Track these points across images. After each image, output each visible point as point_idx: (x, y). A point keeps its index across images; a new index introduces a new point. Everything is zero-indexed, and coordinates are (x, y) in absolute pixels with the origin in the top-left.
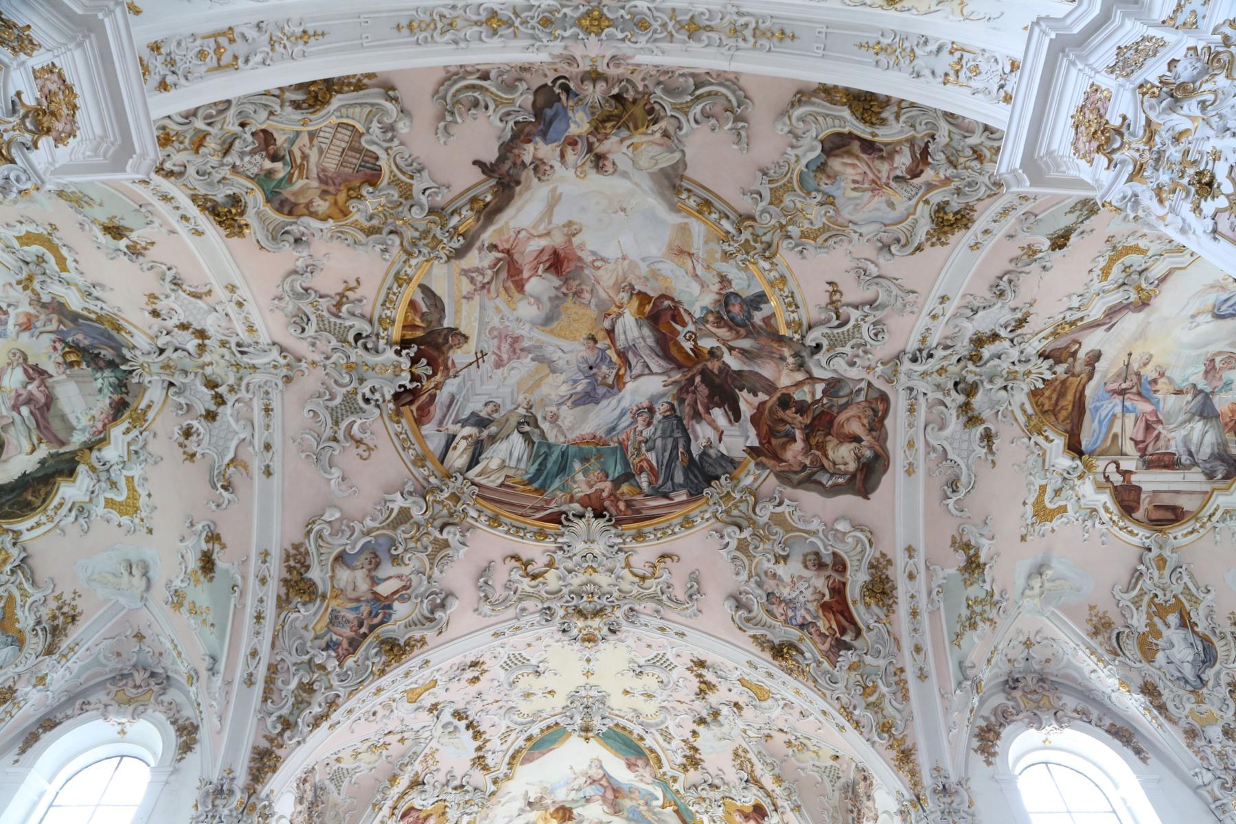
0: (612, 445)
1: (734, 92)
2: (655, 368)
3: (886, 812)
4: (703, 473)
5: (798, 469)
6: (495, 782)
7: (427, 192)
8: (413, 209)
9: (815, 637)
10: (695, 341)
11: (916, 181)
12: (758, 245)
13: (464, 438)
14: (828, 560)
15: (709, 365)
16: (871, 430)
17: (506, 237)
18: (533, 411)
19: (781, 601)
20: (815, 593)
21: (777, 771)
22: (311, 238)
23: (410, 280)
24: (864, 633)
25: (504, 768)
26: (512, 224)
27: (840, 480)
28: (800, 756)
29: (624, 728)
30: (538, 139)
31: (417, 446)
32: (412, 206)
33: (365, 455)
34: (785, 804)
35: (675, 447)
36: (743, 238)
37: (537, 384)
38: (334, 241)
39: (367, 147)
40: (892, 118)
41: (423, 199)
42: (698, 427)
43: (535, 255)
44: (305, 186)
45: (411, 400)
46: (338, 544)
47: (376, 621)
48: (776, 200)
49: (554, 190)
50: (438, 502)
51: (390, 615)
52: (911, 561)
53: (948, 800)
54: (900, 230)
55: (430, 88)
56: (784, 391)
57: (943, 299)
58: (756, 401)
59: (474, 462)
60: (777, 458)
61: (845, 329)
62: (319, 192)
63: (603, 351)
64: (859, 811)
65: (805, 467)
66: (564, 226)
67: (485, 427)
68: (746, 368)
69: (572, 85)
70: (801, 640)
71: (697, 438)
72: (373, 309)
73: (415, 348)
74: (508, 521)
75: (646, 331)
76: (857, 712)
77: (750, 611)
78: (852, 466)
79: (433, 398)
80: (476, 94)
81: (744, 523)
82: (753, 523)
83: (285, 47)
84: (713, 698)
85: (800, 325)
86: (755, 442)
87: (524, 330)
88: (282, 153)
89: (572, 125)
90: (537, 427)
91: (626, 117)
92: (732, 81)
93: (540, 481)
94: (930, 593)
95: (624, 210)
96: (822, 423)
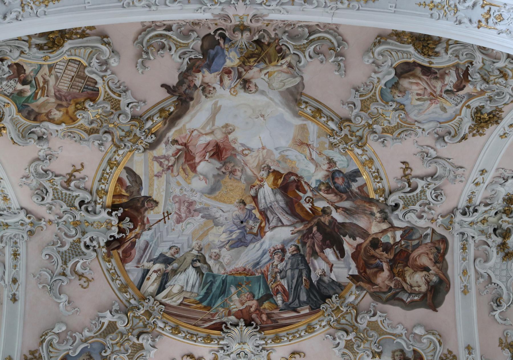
0: (257, 275)
1: (335, 37)
4: (320, 294)
5: (385, 290)
7: (130, 106)
8: (121, 117)
10: (312, 203)
11: (461, 93)
12: (353, 138)
13: (155, 271)
15: (322, 219)
16: (436, 262)
17: (184, 135)
18: (203, 252)
22: (50, 136)
23: (119, 164)
26: (188, 126)
27: (416, 298)
30: (204, 70)
31: (122, 278)
32: (120, 115)
33: (85, 285)
35: (300, 276)
36: (343, 133)
37: (205, 234)
38: (66, 138)
39: (89, 75)
40: (442, 51)
41: (128, 110)
42: (315, 262)
43: (204, 146)
44: (45, 101)
45: (118, 246)
48: (365, 108)
49: (216, 104)
50: (136, 317)
54: (450, 126)
55: (132, 37)
56: (374, 236)
57: (483, 172)
58: (355, 243)
59: (162, 288)
61: (415, 193)
62: (55, 105)
63: (250, 211)
65: (390, 289)
66: (223, 127)
67: (170, 264)
68: (347, 221)
69: (227, 34)
71: (315, 269)
72: (93, 184)
73: (121, 210)
74: (185, 329)
75: (279, 197)
78: (424, 288)
79: (133, 244)
80: (163, 41)
81: (350, 329)
82: (355, 329)
83: (32, 8)
85: (384, 191)
86: (354, 271)
87: (196, 198)
88: (30, 79)
89: (228, 60)
90: (205, 263)
91: (263, 55)
92: (334, 30)
95: (263, 116)
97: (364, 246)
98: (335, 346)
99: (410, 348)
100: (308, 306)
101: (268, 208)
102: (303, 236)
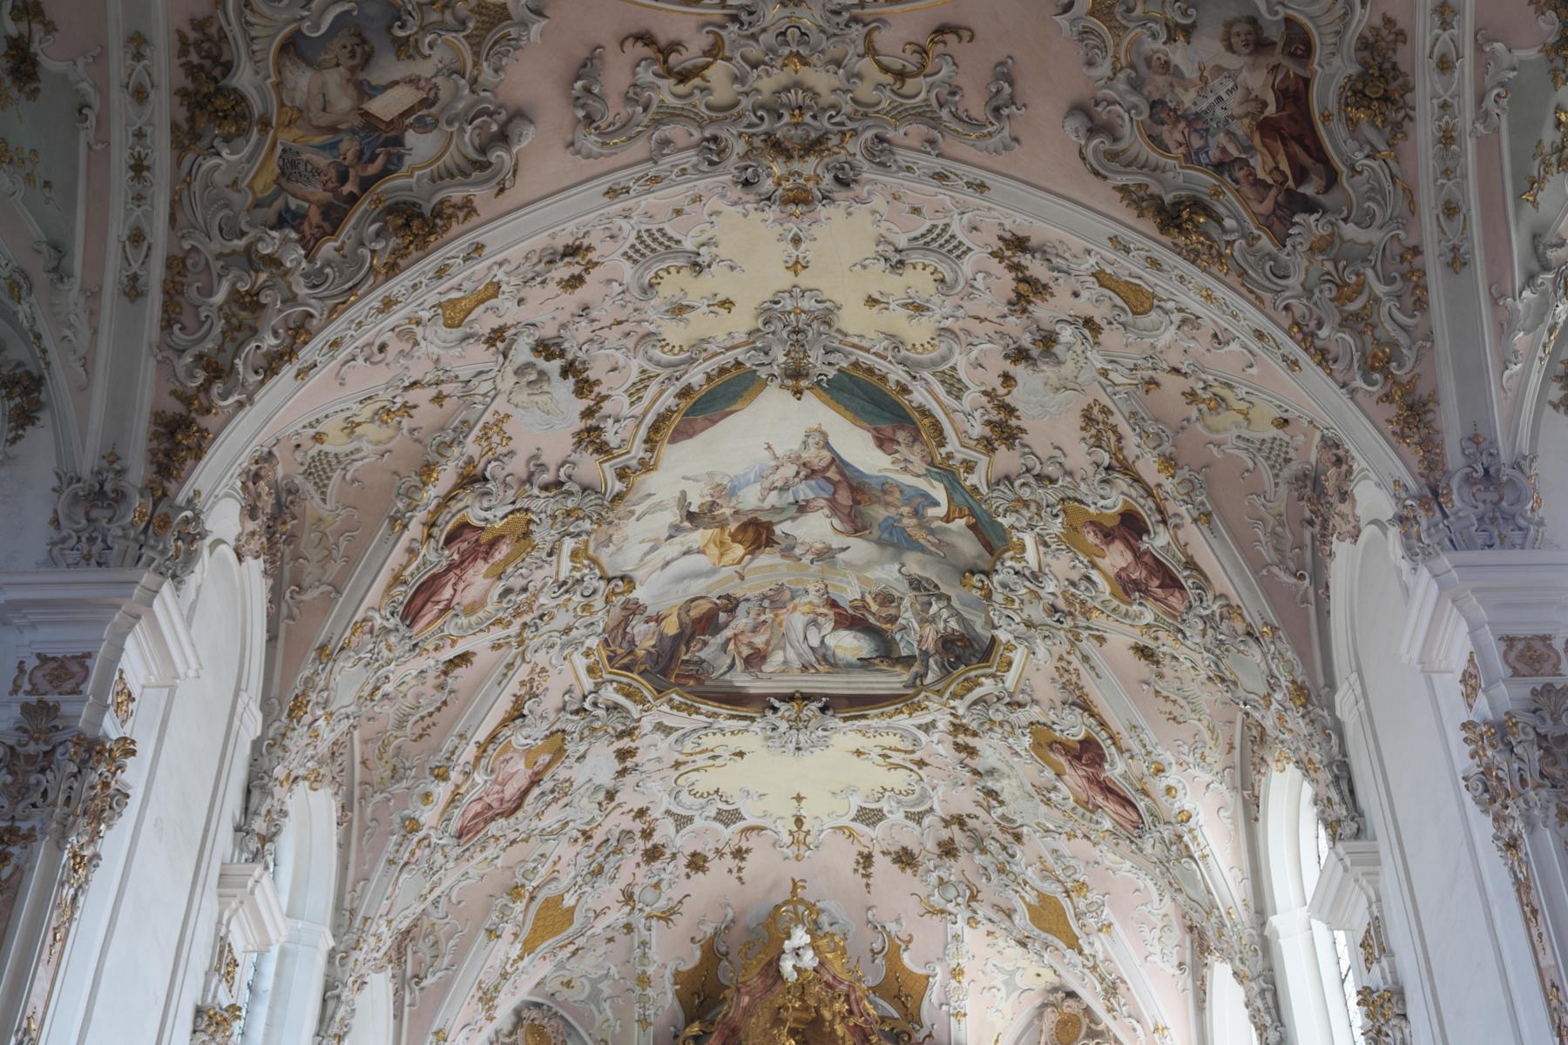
3: (1374, 522)
6: (622, 474)
14: (1275, 34)
19: (1177, 116)
20: (1246, 100)
24: (1344, 180)
25: (638, 450)
28: (1212, 420)
29: (870, 371)
34: (1183, 510)
47: (372, 169)
51: (400, 157)
52: (1446, 36)
64: (1326, 521)
76: (1323, 333)
77: (1116, 140)
84: (1043, 311)
94: (1480, 98)
98: (1060, 10)
99: (1277, 13)
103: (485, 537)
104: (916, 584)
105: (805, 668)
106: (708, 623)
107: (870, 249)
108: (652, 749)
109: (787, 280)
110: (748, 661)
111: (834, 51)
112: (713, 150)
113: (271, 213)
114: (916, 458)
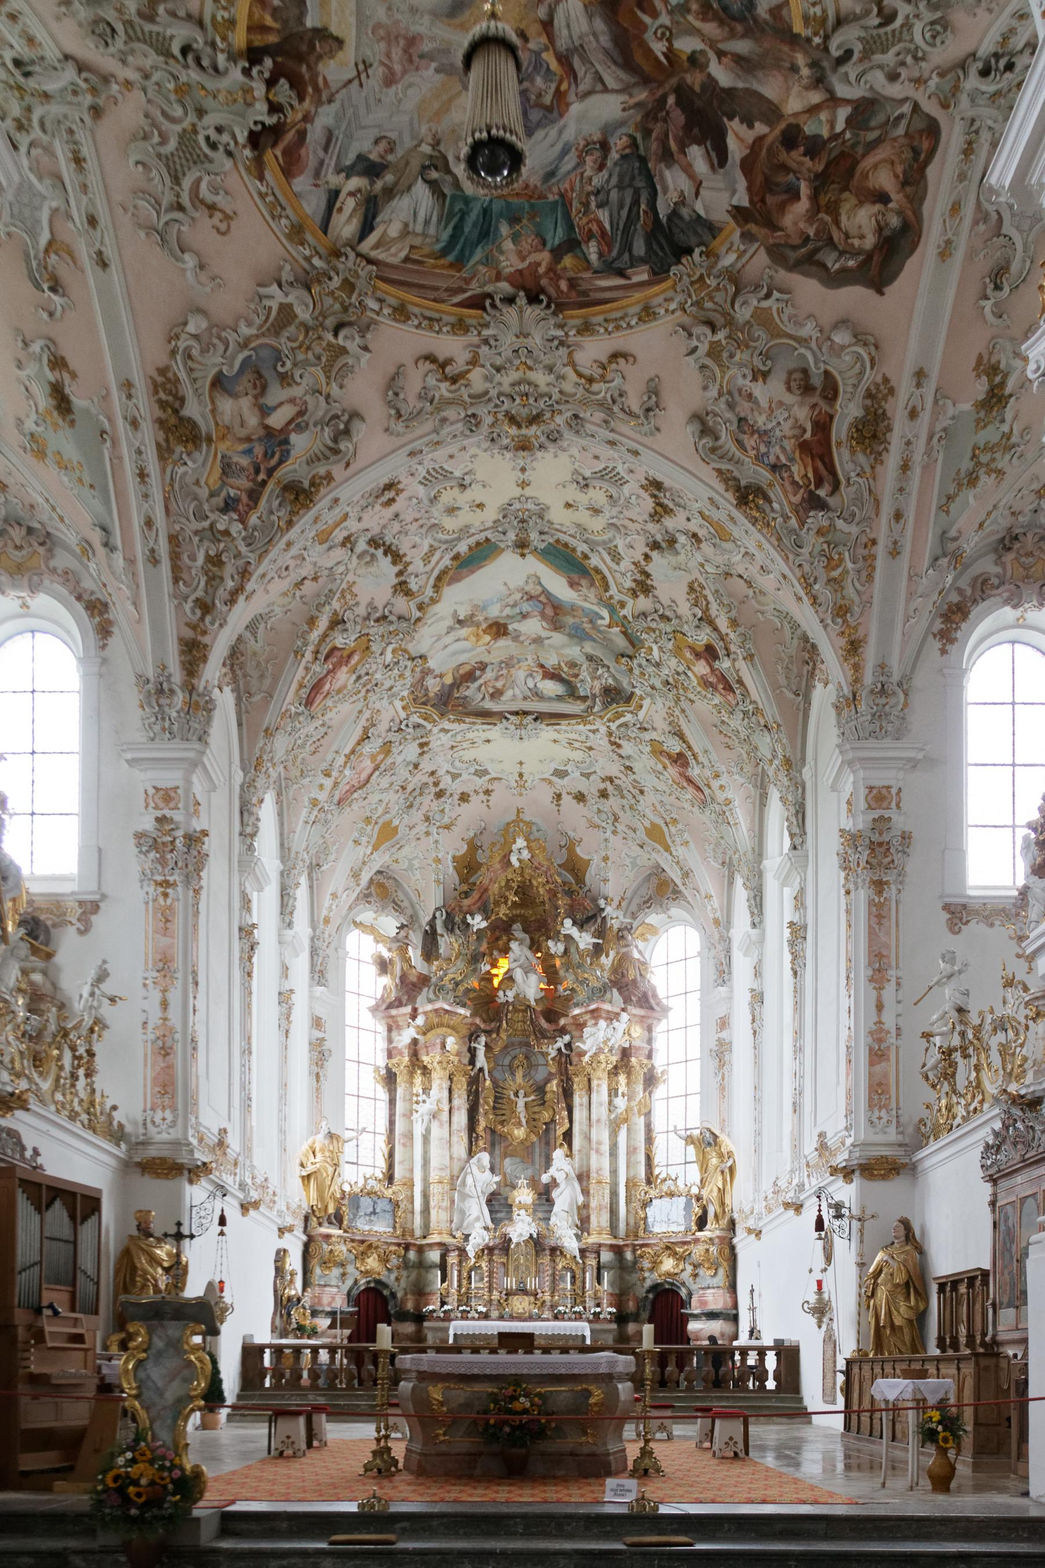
0: (551, 198)
2: (610, 82)
4: (671, 242)
5: (796, 241)
6: (421, 607)
9: (787, 484)
10: (669, 40)
13: (351, 194)
14: (817, 381)
15: (689, 78)
16: (905, 183)
18: (442, 148)
19: (754, 431)
21: (733, 614)
25: (429, 592)
27: (851, 263)
29: (566, 545)
31: (289, 211)
33: (223, 227)
35: (636, 203)
37: (446, 108)
42: (667, 174)
46: (213, 362)
53: (883, 701)
56: (792, 120)
58: (749, 136)
59: (367, 228)
60: (772, 225)
61: (889, 29)
63: (538, 54)
65: (807, 239)
67: (378, 175)
68: (740, 85)
70: (770, 485)
71: (665, 190)
73: (268, 62)
74: (416, 310)
75: (599, 24)
78: (870, 242)
79: (302, 135)
81: (719, 320)
82: (730, 322)
84: (669, 523)
85: (824, 20)
86: (742, 199)
87: (422, 26)
90: (448, 171)
93: (455, 253)
96: (839, 172)
97: (769, 140)
100: (646, 267)
101: (576, 49)
102: (646, 116)
103: (345, 653)
104: (590, 658)
105: (525, 698)
106: (470, 677)
107: (569, 478)
108: (439, 740)
109: (517, 492)
110: (492, 696)
111: (547, 360)
112: (473, 421)
113: (219, 501)
114: (592, 595)
